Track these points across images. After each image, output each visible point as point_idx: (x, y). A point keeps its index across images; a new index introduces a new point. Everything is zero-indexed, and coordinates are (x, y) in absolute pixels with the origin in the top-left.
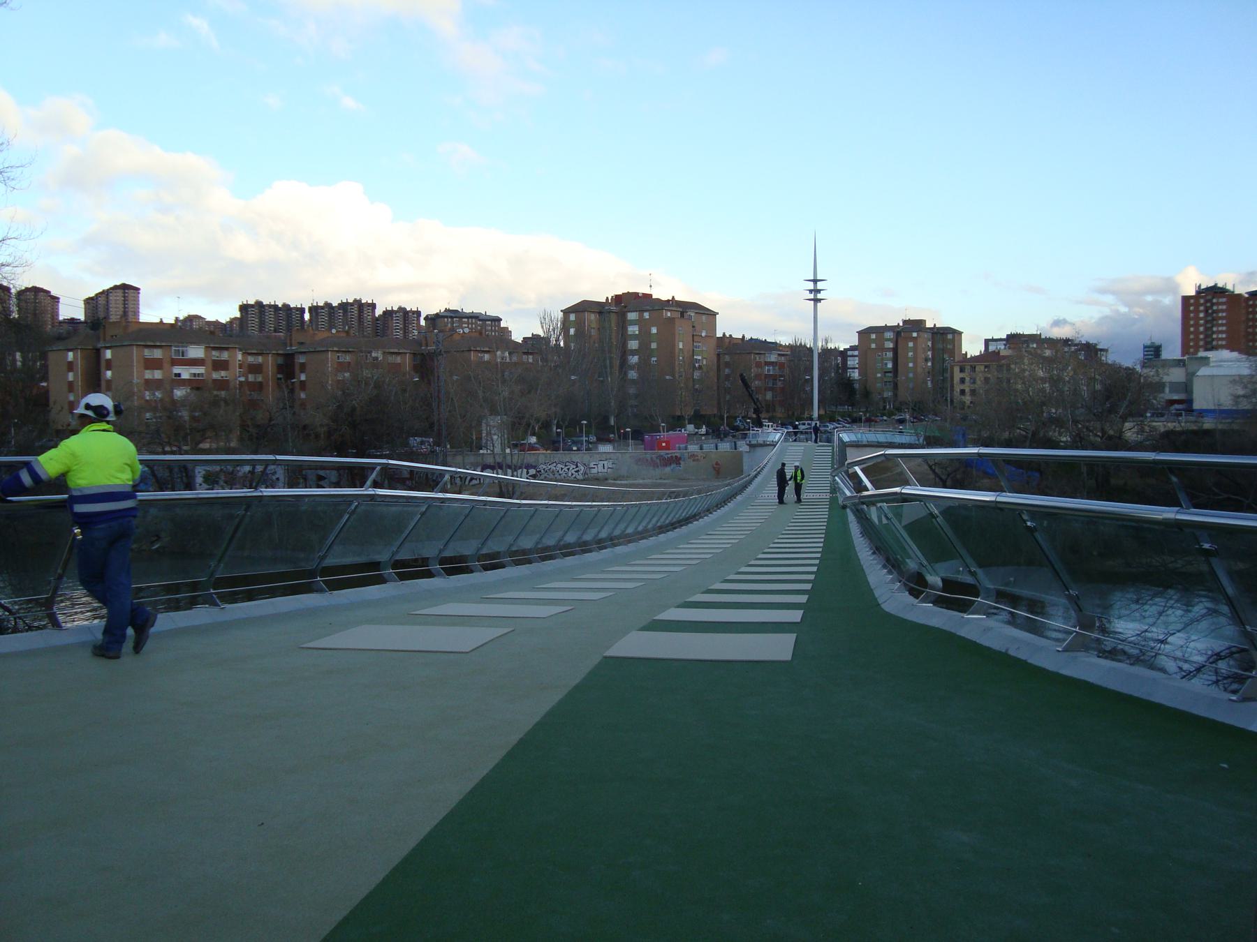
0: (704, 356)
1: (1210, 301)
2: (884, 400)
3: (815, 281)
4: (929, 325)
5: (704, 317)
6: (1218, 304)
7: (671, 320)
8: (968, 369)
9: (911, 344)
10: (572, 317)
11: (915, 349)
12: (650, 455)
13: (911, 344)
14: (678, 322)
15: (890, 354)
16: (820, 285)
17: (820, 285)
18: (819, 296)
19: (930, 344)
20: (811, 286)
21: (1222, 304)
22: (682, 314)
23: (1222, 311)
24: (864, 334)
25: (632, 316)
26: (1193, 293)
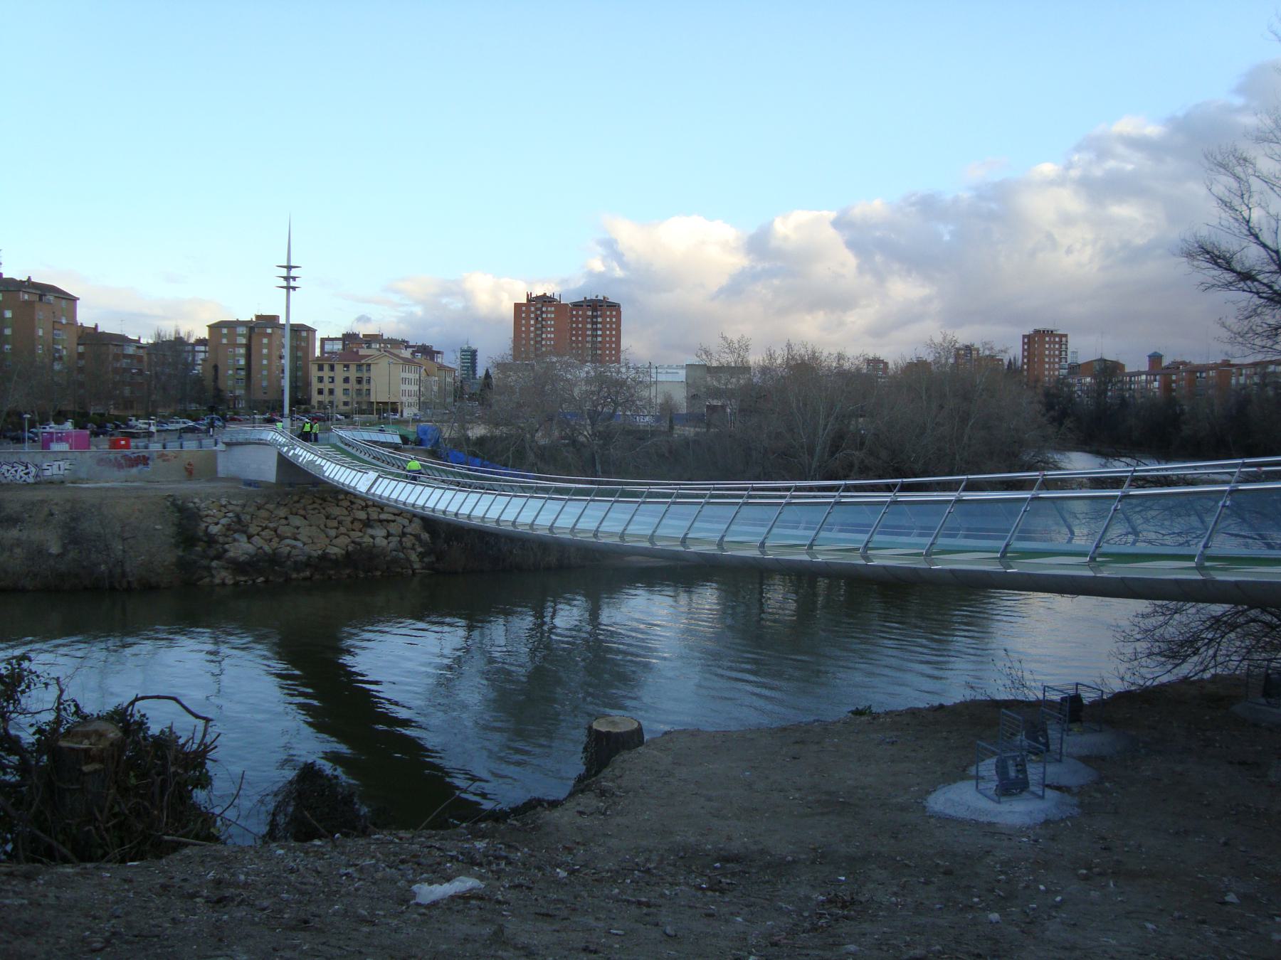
0: (67, 346)
1: (540, 309)
2: (236, 398)
3: (289, 268)
5: (64, 303)
6: (547, 312)
7: (30, 304)
8: (326, 368)
11: (269, 346)
12: (115, 454)
13: (265, 341)
14: (38, 306)
15: (242, 351)
16: (294, 273)
17: (294, 273)
18: (292, 284)
20: (284, 272)
22: (41, 299)
23: (551, 319)
24: (215, 328)
26: (525, 301)
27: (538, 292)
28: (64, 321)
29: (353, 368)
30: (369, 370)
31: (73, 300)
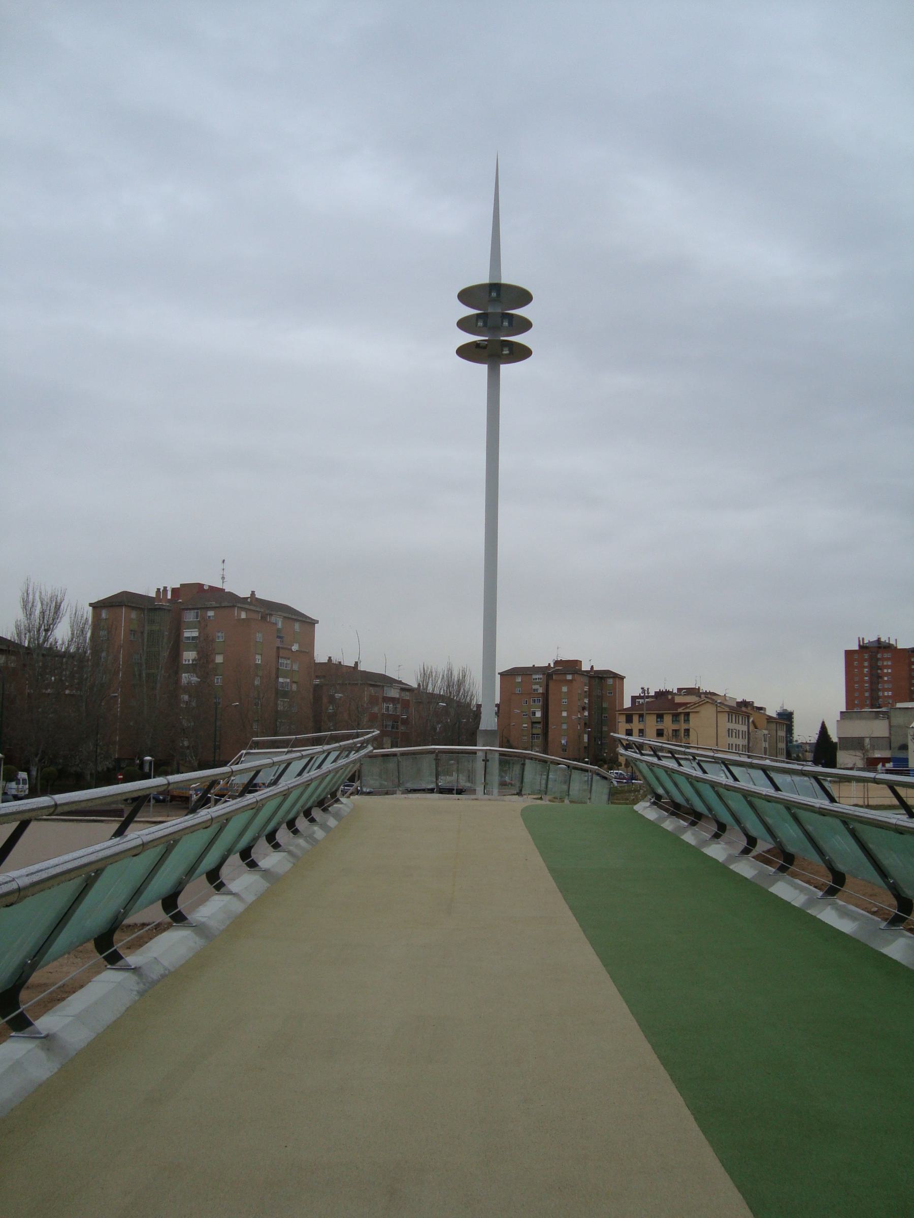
4: (585, 667)
5: (297, 626)
6: (883, 659)
9: (565, 689)
10: (104, 614)
11: (569, 691)
13: (565, 689)
19: (586, 688)
21: (888, 659)
22: (264, 618)
25: (190, 617)
26: (857, 648)
27: (870, 638)
28: (295, 648)
29: (668, 719)
30: (687, 720)
31: (309, 623)
